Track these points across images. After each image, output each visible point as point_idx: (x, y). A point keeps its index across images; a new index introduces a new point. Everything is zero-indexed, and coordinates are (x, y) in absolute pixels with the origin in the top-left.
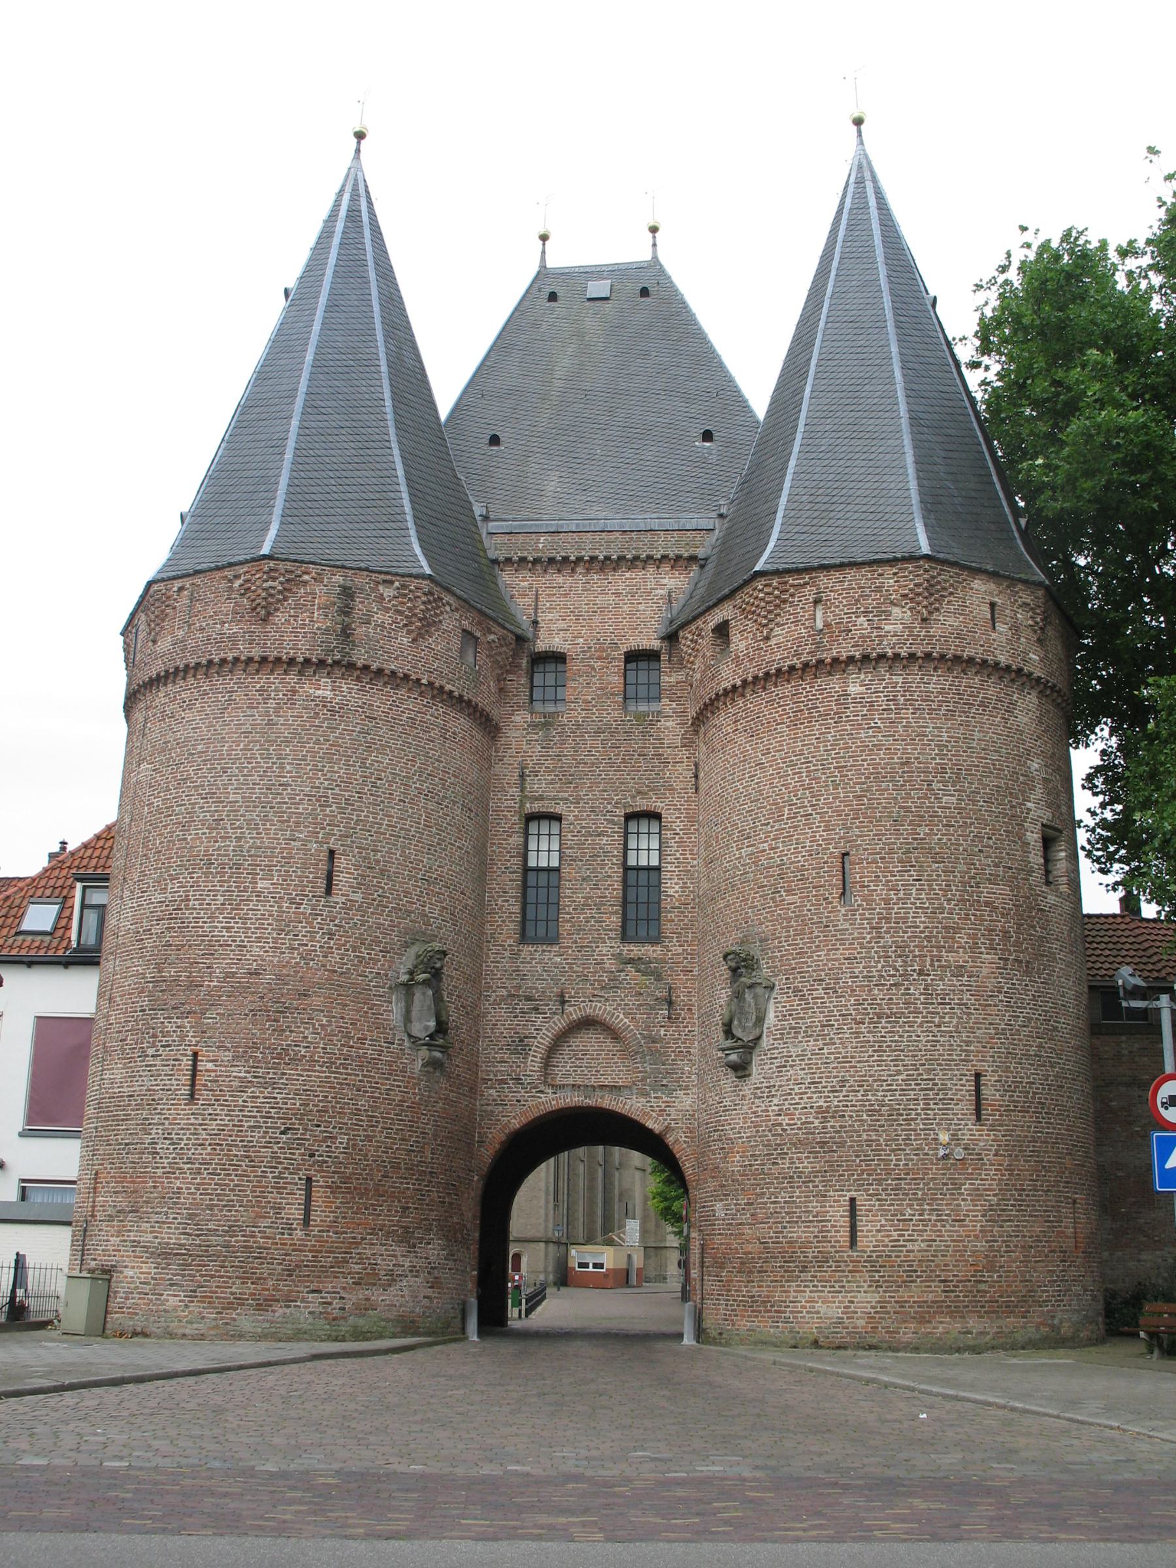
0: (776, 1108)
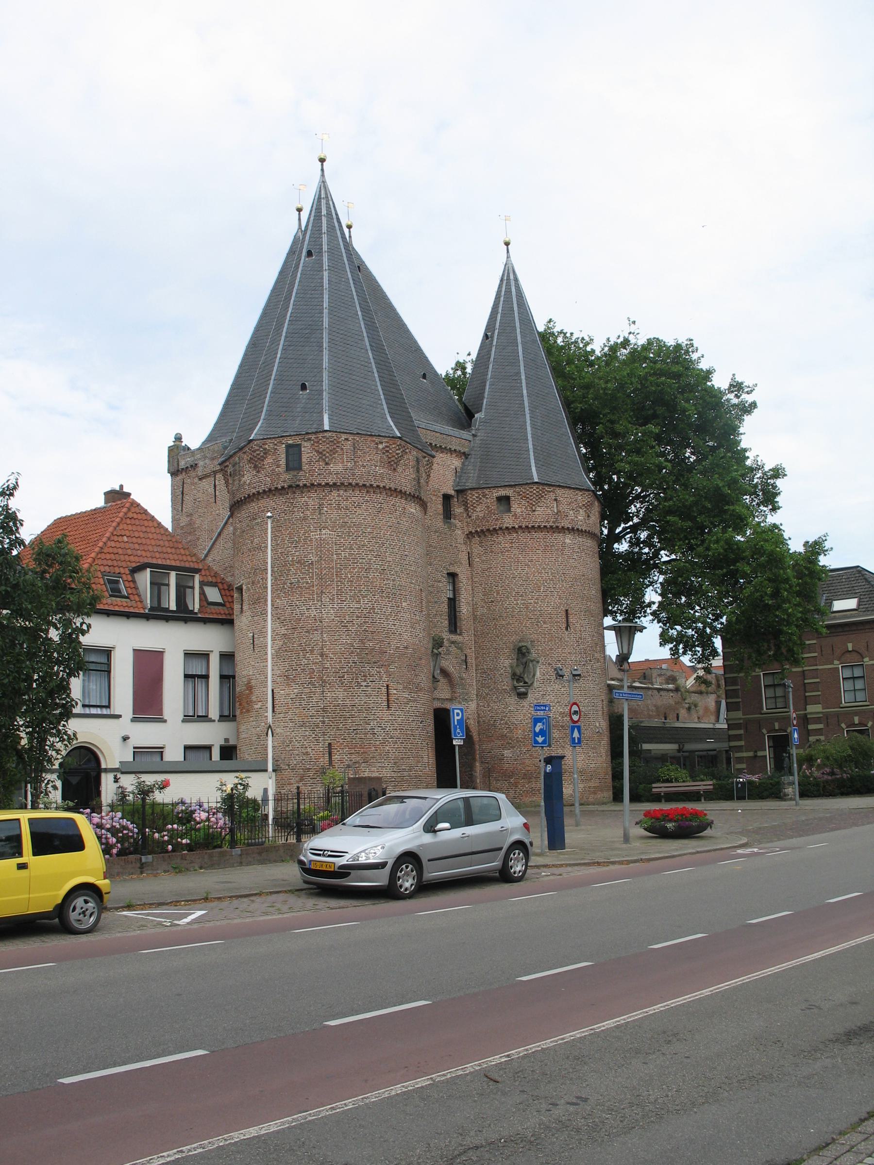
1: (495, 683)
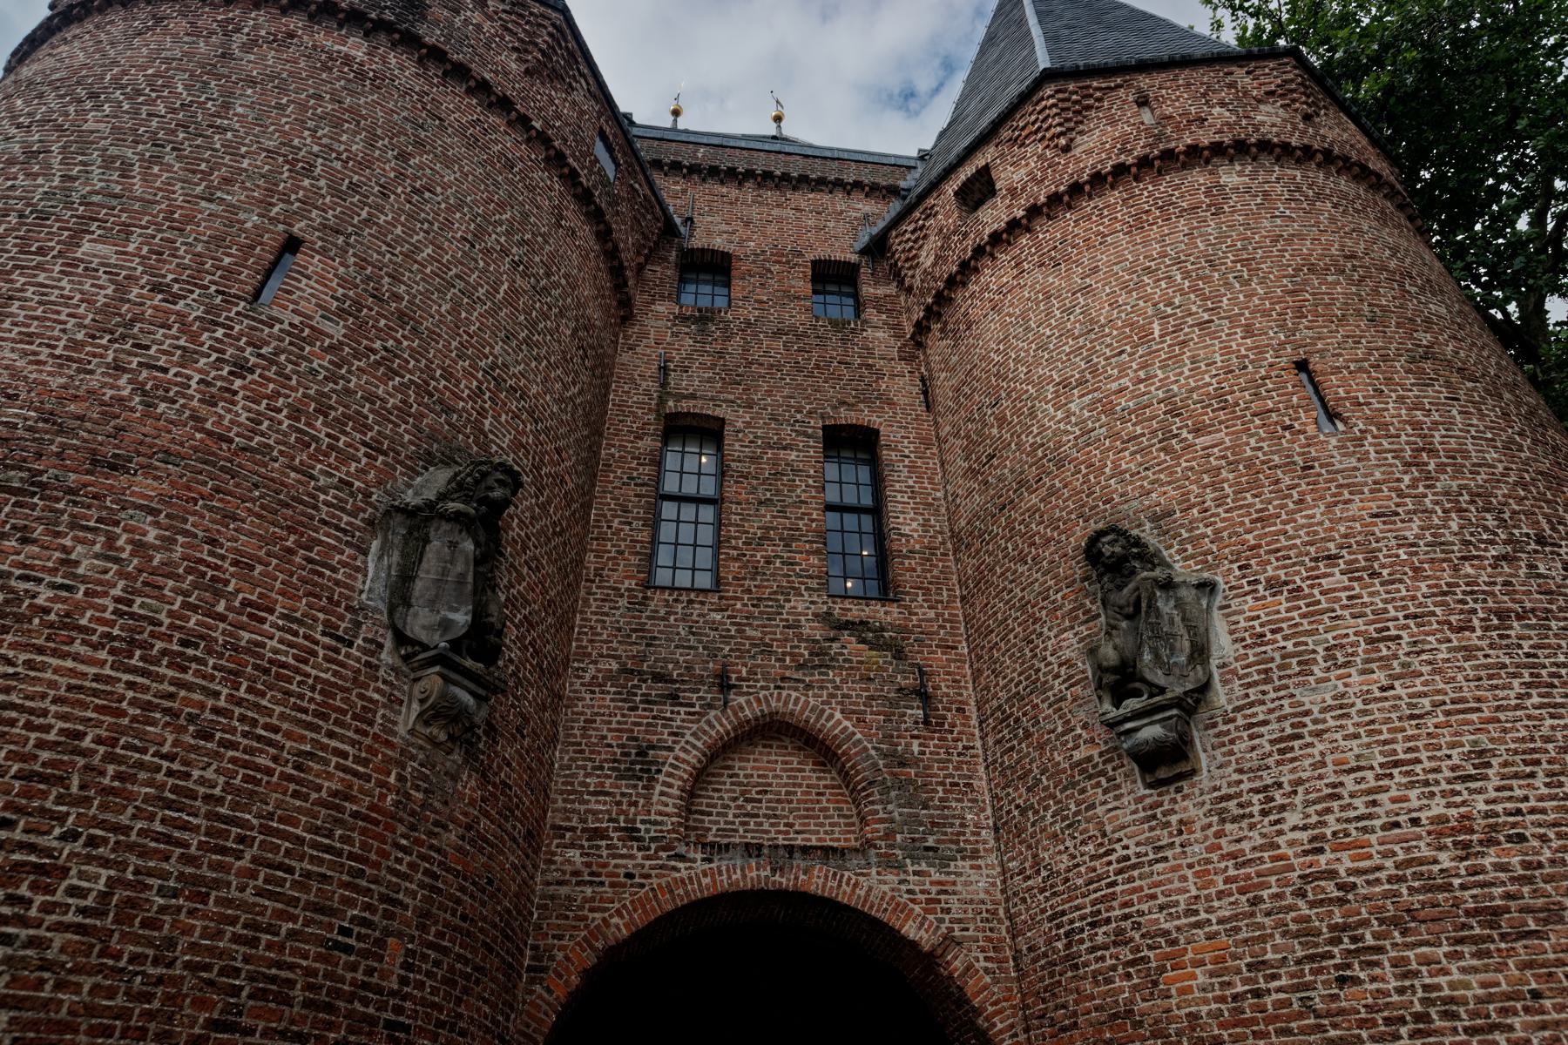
0: (1304, 836)
1: (1041, 747)
